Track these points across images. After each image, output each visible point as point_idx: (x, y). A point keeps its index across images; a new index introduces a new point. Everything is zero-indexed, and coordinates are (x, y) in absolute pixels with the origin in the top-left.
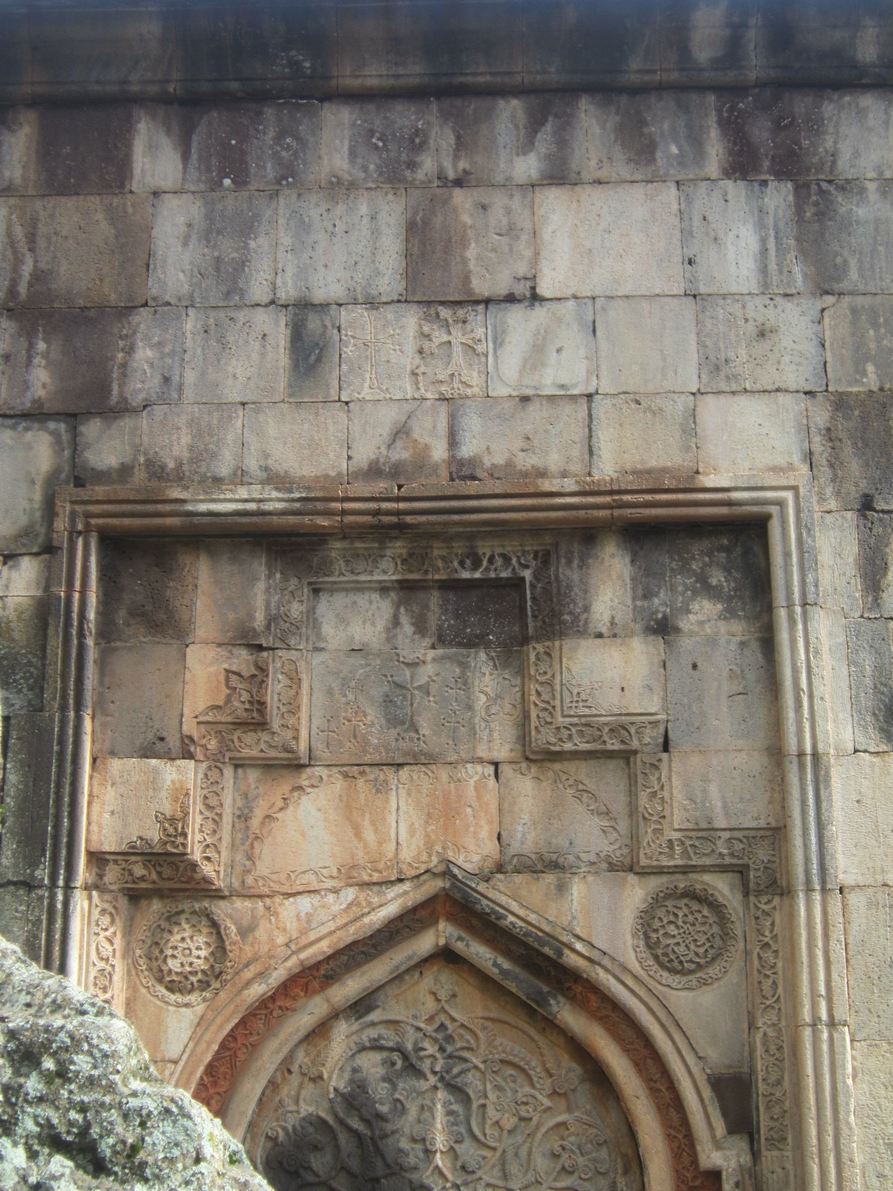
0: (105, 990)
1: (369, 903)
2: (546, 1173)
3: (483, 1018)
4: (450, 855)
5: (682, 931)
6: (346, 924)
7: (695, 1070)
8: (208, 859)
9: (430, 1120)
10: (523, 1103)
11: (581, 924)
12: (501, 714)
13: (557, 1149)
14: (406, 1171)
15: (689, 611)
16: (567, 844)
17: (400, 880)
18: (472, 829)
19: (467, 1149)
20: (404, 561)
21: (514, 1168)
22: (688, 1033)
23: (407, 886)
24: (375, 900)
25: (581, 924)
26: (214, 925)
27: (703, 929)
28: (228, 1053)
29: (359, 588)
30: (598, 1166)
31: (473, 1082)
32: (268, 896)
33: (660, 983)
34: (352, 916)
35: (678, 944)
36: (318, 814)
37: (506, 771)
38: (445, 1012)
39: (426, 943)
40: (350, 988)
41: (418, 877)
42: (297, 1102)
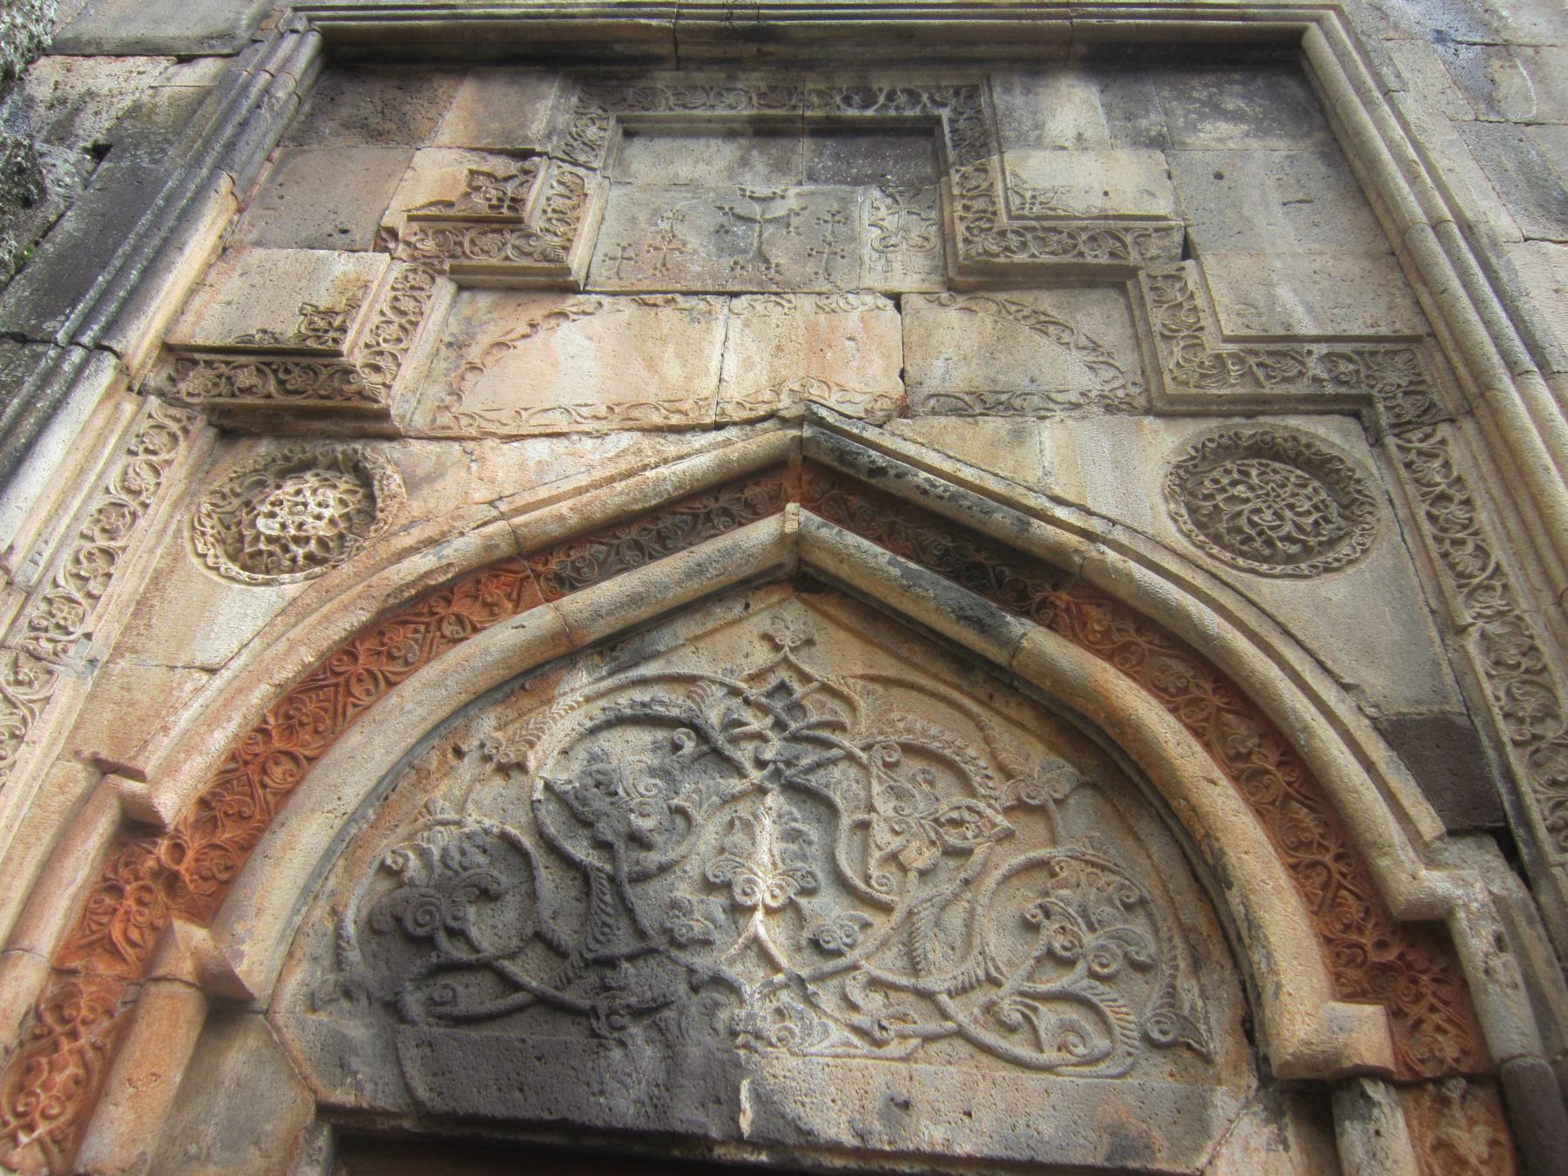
2: (1010, 963)
3: (863, 677)
4: (815, 392)
6: (611, 480)
8: (377, 369)
9: (747, 844)
11: (1063, 480)
12: (904, 246)
13: (1031, 909)
14: (681, 946)
15: (1195, 130)
16: (1027, 380)
17: (718, 426)
18: (853, 364)
19: (829, 909)
20: (761, 95)
21: (932, 949)
22: (1313, 645)
25: (1063, 480)
29: (692, 130)
30: (1132, 950)
31: (840, 783)
32: (473, 439)
34: (623, 466)
35: (1258, 511)
36: (588, 343)
37: (913, 302)
38: (792, 667)
39: (760, 533)
40: (605, 596)
41: (751, 422)
42: (462, 808)
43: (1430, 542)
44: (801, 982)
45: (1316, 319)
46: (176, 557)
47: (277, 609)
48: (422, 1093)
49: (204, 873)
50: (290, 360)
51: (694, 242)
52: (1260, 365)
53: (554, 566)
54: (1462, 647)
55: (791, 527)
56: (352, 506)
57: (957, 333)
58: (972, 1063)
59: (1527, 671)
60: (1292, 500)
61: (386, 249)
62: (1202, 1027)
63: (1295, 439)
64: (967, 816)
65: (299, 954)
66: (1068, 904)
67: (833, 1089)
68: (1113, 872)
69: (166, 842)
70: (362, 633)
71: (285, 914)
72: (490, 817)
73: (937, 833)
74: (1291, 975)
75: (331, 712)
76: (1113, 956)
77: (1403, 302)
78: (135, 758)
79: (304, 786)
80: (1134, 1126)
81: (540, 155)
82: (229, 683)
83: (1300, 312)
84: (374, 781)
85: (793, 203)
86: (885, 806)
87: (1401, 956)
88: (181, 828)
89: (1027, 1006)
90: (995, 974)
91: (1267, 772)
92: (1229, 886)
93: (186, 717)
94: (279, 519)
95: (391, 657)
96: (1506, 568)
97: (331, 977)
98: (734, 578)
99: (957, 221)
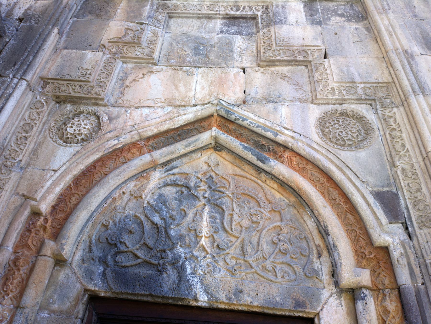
0: (26, 132)
1: (178, 113)
7: (361, 188)
9: (200, 220)
13: (275, 240)
15: (330, 20)
17: (195, 106)
18: (231, 88)
21: (249, 249)
22: (354, 170)
23: (198, 107)
24: (182, 112)
26: (98, 117)
36: (159, 81)
37: (248, 70)
41: (204, 105)
43: (389, 141)
45: (361, 77)
46: (45, 139)
47: (73, 154)
50: (76, 83)
51: (188, 52)
53: (150, 143)
54: (396, 171)
55: (214, 134)
57: (260, 80)
59: (414, 179)
60: (351, 129)
61: (102, 51)
62: (320, 273)
63: (353, 111)
64: (258, 213)
65: (79, 248)
66: (285, 238)
69: (43, 218)
70: (97, 161)
71: (76, 238)
73: (250, 217)
74: (345, 260)
77: (386, 72)
78: (34, 195)
79: (81, 203)
80: (302, 299)
81: (145, 24)
82: (60, 175)
83: (356, 75)
84: (100, 201)
85: (216, 40)
86: (236, 210)
87: (375, 256)
88: (47, 214)
89: (273, 265)
90: (265, 256)
91: (341, 204)
92: (329, 235)
93: (48, 184)
94: (73, 128)
96: (409, 150)
98: (198, 147)
99: (261, 46)
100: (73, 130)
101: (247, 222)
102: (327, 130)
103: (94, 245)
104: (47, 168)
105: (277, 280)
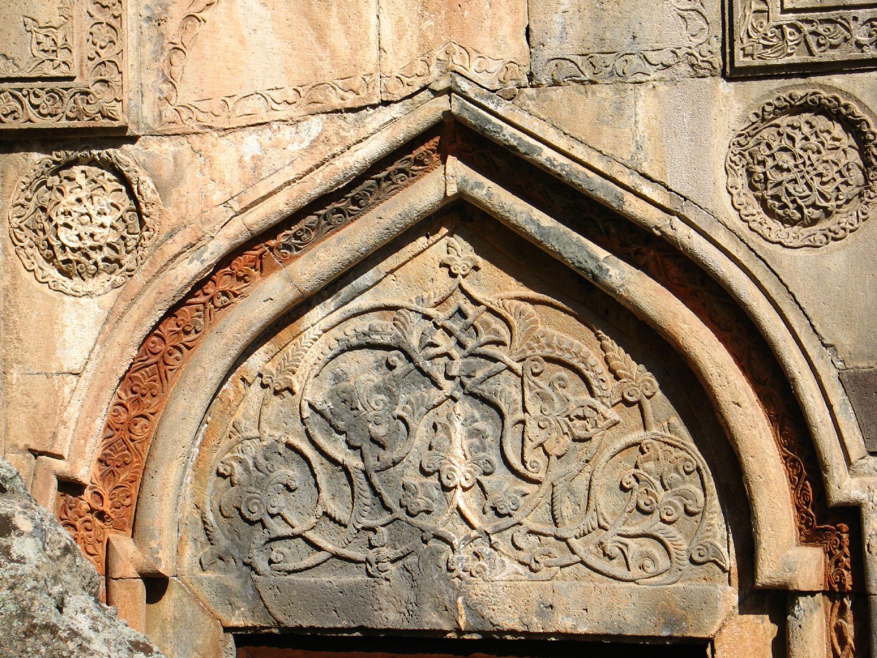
4: (457, 62)
5: (800, 161)
9: (447, 443)
10: (578, 417)
16: (629, 40)
17: (386, 103)
18: (488, 23)
21: (566, 509)
23: (395, 110)
25: (650, 157)
27: (831, 157)
28: (154, 359)
32: (197, 133)
33: (766, 239)
34: (318, 159)
35: (795, 181)
36: (263, 11)
38: (464, 291)
44: (488, 534)
46: (15, 276)
48: (280, 617)
49: (117, 505)
52: (814, 33)
56: (122, 209)
58: (590, 578)
64: (587, 414)
67: (509, 600)
68: (681, 449)
72: (277, 429)
73: (568, 426)
75: (158, 379)
76: (676, 508)
78: (52, 446)
88: (94, 481)
89: (622, 543)
90: (603, 523)
95: (187, 333)
97: (208, 549)
100: (77, 238)
101: (561, 439)
102: (759, 169)
103: (215, 525)
104: (54, 367)
105: (629, 575)
